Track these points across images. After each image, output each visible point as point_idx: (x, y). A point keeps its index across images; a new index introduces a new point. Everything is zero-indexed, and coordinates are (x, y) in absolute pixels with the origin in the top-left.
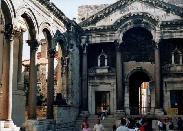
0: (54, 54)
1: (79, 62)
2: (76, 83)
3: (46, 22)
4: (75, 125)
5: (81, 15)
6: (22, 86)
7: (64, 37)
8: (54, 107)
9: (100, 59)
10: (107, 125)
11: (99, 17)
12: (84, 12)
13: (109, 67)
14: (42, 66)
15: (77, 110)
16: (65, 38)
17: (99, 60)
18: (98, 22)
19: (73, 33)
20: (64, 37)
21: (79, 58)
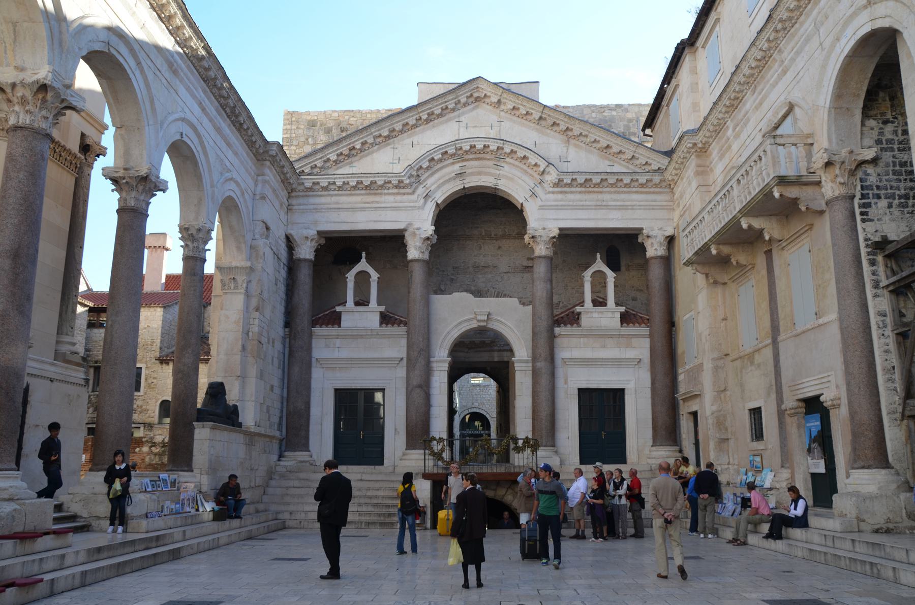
0: (206, 243)
1: (282, 288)
2: (273, 358)
3: (182, 115)
4: (265, 497)
5: (292, 148)
6: (74, 349)
7: (243, 194)
8: (197, 431)
9: (356, 283)
10: (376, 497)
11: (358, 146)
12: (303, 139)
13: (382, 308)
14: (149, 314)
15: (276, 446)
16: (245, 201)
17: (351, 286)
18: (354, 164)
19: (271, 186)
20: (243, 194)
21: (283, 273)
